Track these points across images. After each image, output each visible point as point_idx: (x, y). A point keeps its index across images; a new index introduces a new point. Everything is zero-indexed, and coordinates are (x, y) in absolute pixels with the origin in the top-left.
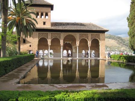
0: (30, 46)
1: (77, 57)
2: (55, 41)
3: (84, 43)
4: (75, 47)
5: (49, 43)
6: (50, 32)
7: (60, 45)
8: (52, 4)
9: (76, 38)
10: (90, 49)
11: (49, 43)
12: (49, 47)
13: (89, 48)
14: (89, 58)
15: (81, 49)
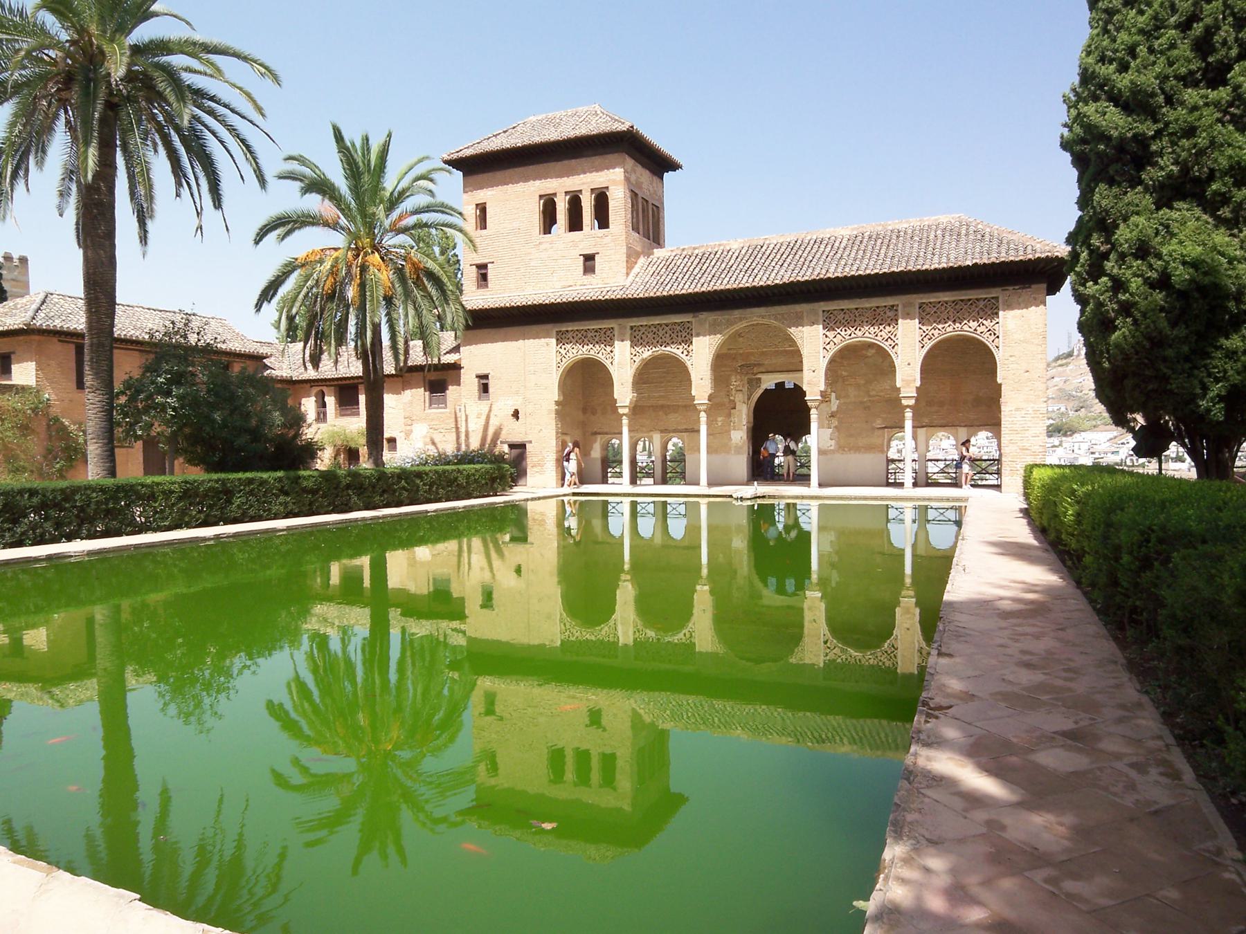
0: (516, 414)
1: (809, 485)
2: (662, 378)
3: (861, 367)
4: (833, 415)
5: (624, 394)
6: (621, 321)
7: (693, 398)
8: (624, 128)
9: (799, 342)
10: (914, 419)
11: (624, 394)
12: (625, 421)
13: (909, 414)
14: (909, 491)
15: (879, 423)
